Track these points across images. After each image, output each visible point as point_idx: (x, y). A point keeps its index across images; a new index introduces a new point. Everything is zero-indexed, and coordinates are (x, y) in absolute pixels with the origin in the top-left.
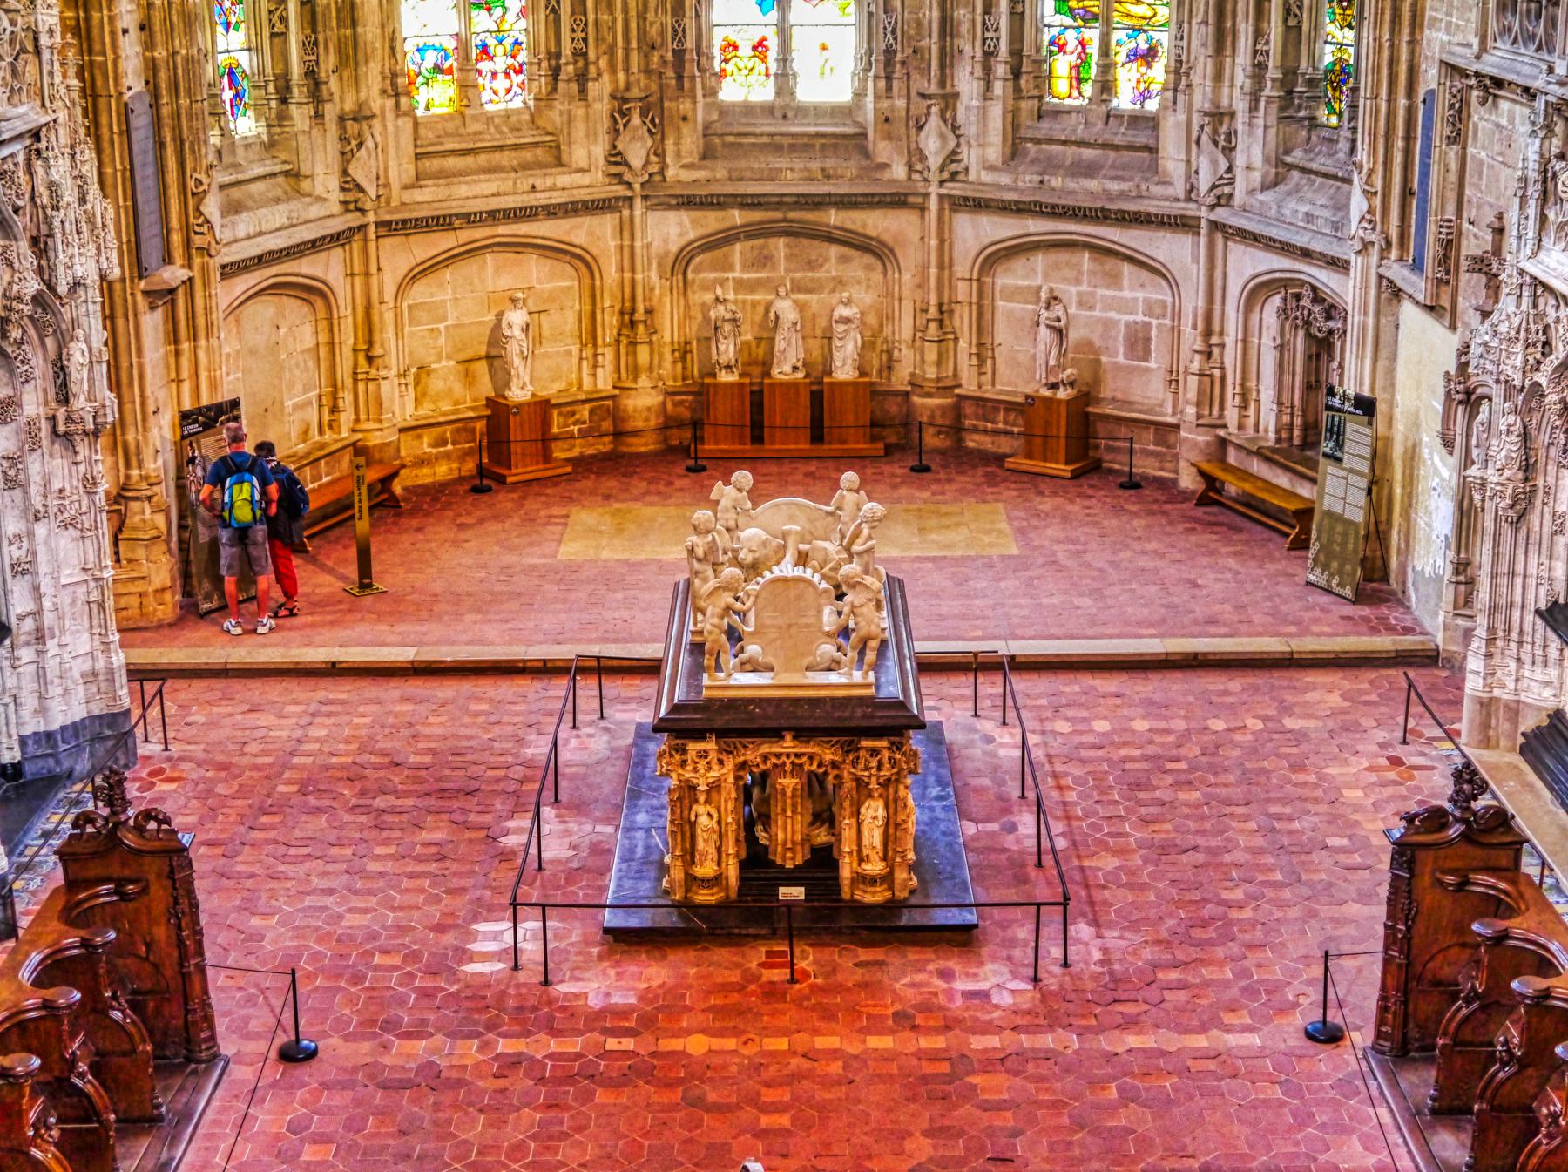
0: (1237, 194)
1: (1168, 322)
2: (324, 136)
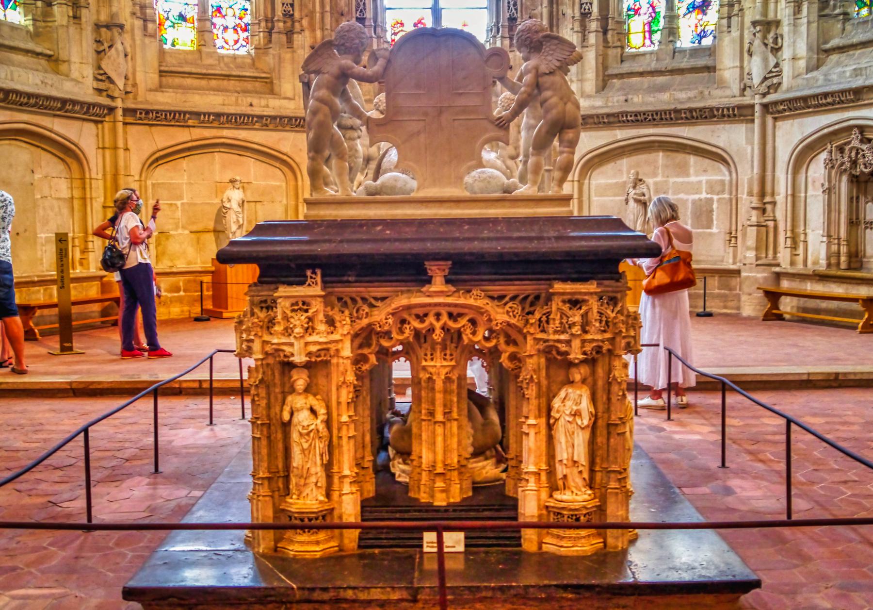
0: (785, 80)
1: (726, 196)
2: (81, 34)
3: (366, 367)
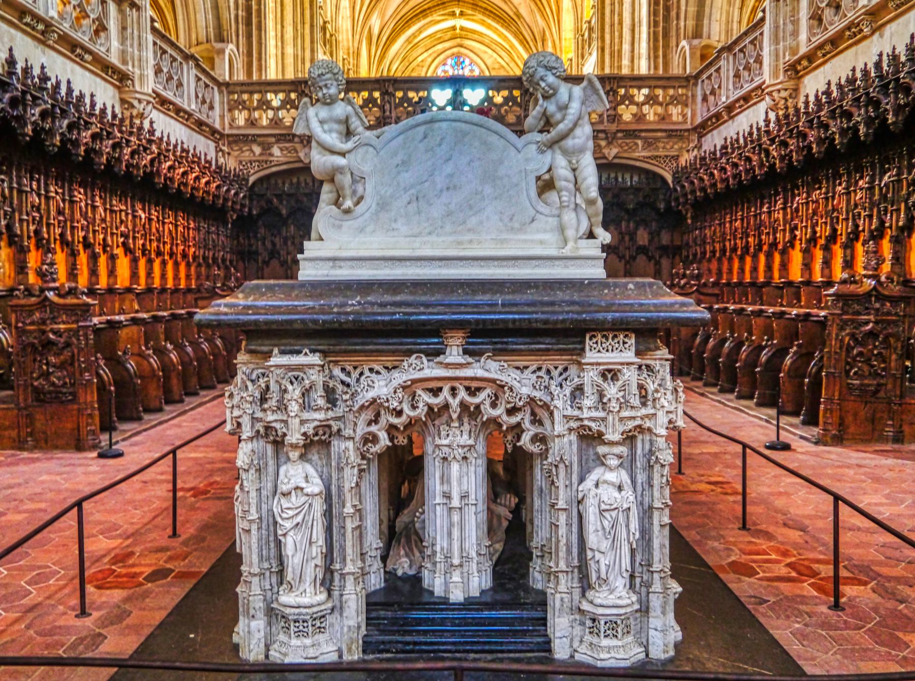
3: (376, 449)
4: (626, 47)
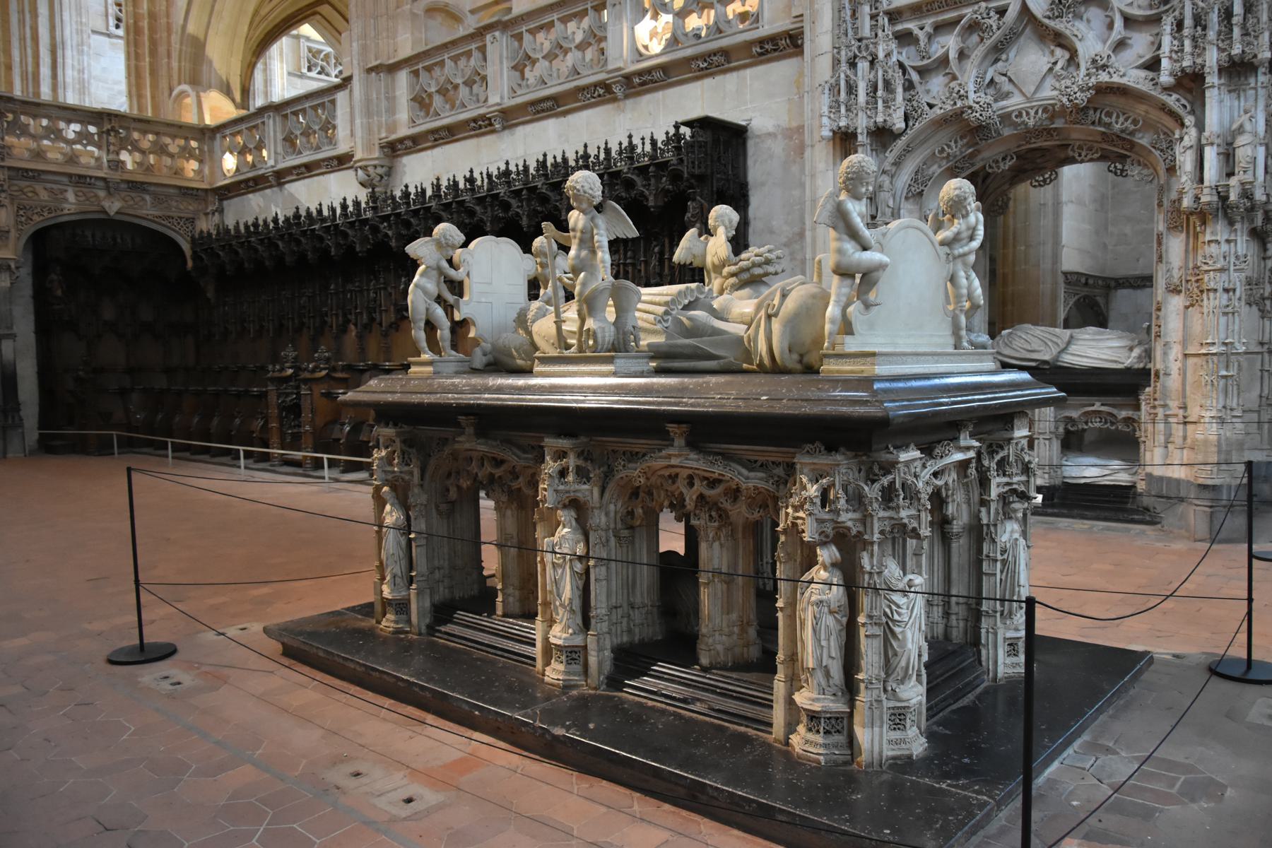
4: (45, 71)
